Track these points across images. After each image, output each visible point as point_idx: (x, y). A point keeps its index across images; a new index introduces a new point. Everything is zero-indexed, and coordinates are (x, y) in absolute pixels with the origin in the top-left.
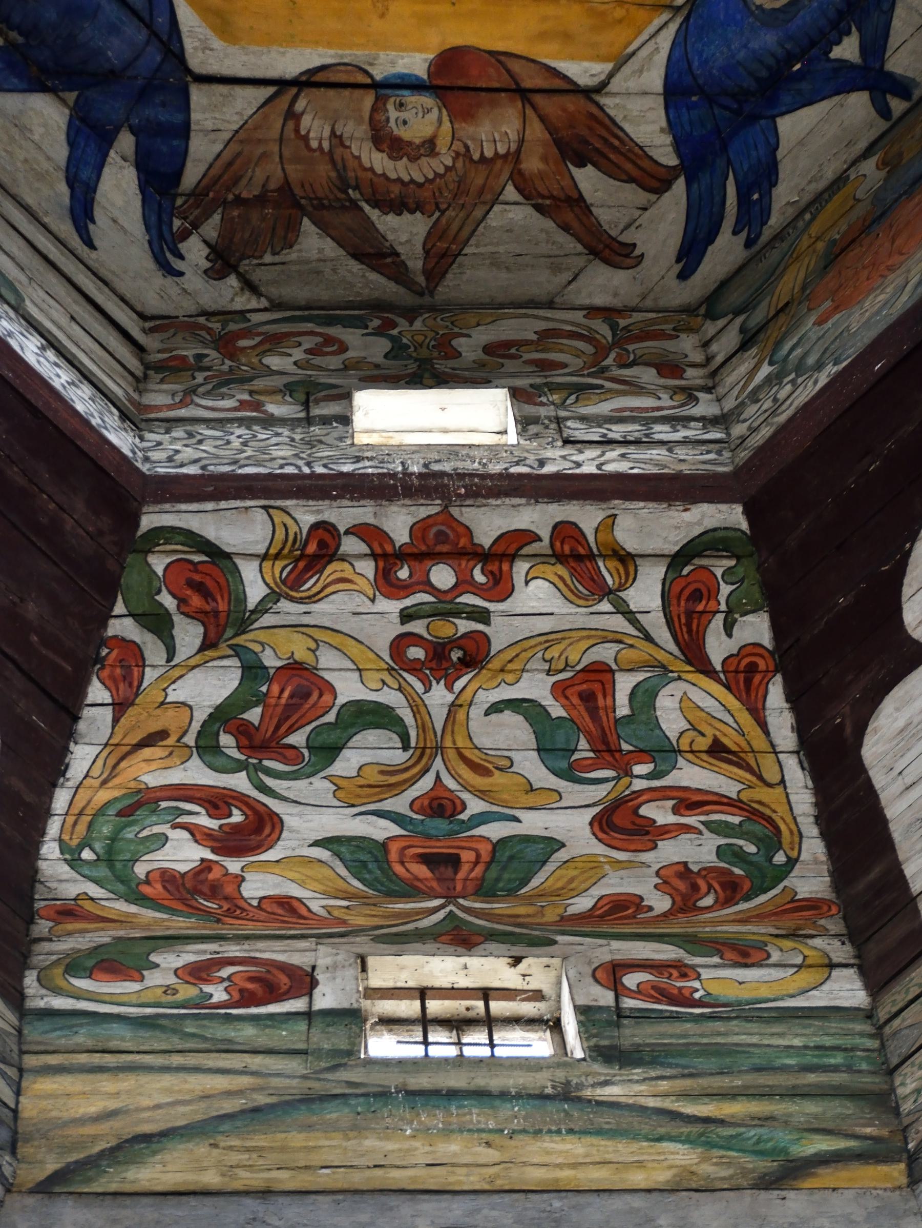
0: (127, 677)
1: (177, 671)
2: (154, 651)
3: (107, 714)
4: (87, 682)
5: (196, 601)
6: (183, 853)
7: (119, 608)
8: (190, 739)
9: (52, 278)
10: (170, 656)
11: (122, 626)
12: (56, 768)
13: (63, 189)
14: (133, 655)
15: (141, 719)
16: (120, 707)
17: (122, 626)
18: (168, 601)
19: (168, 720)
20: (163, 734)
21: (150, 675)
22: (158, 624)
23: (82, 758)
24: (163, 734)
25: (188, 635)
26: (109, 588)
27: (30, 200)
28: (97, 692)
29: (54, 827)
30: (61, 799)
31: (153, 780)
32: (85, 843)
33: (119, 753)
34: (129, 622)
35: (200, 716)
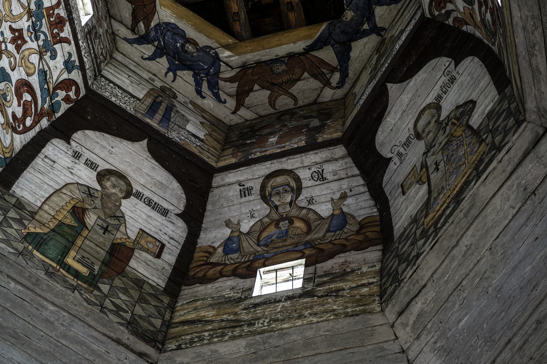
0: (461, 21)
1: (457, 10)
2: (454, 14)
3: (468, 26)
4: (463, 30)
5: (442, 5)
6: (488, 16)
7: (447, 22)
8: (470, 7)
9: (405, 13)
10: (454, 10)
11: (450, 21)
12: (479, 41)
13: (392, 6)
14: (456, 19)
15: (468, 19)
16: (467, 24)
17: (450, 21)
18: (443, 11)
19: (467, 12)
20: (470, 13)
21: (459, 16)
22: (449, 13)
23: (478, 34)
24: (470, 13)
25: (450, 7)
26: (444, 25)
27: (395, 13)
28: (464, 28)
29: (490, 45)
30: (486, 41)
31: (479, 19)
32: (491, 39)
33: (475, 25)
34: (449, 20)
35: (465, 5)
